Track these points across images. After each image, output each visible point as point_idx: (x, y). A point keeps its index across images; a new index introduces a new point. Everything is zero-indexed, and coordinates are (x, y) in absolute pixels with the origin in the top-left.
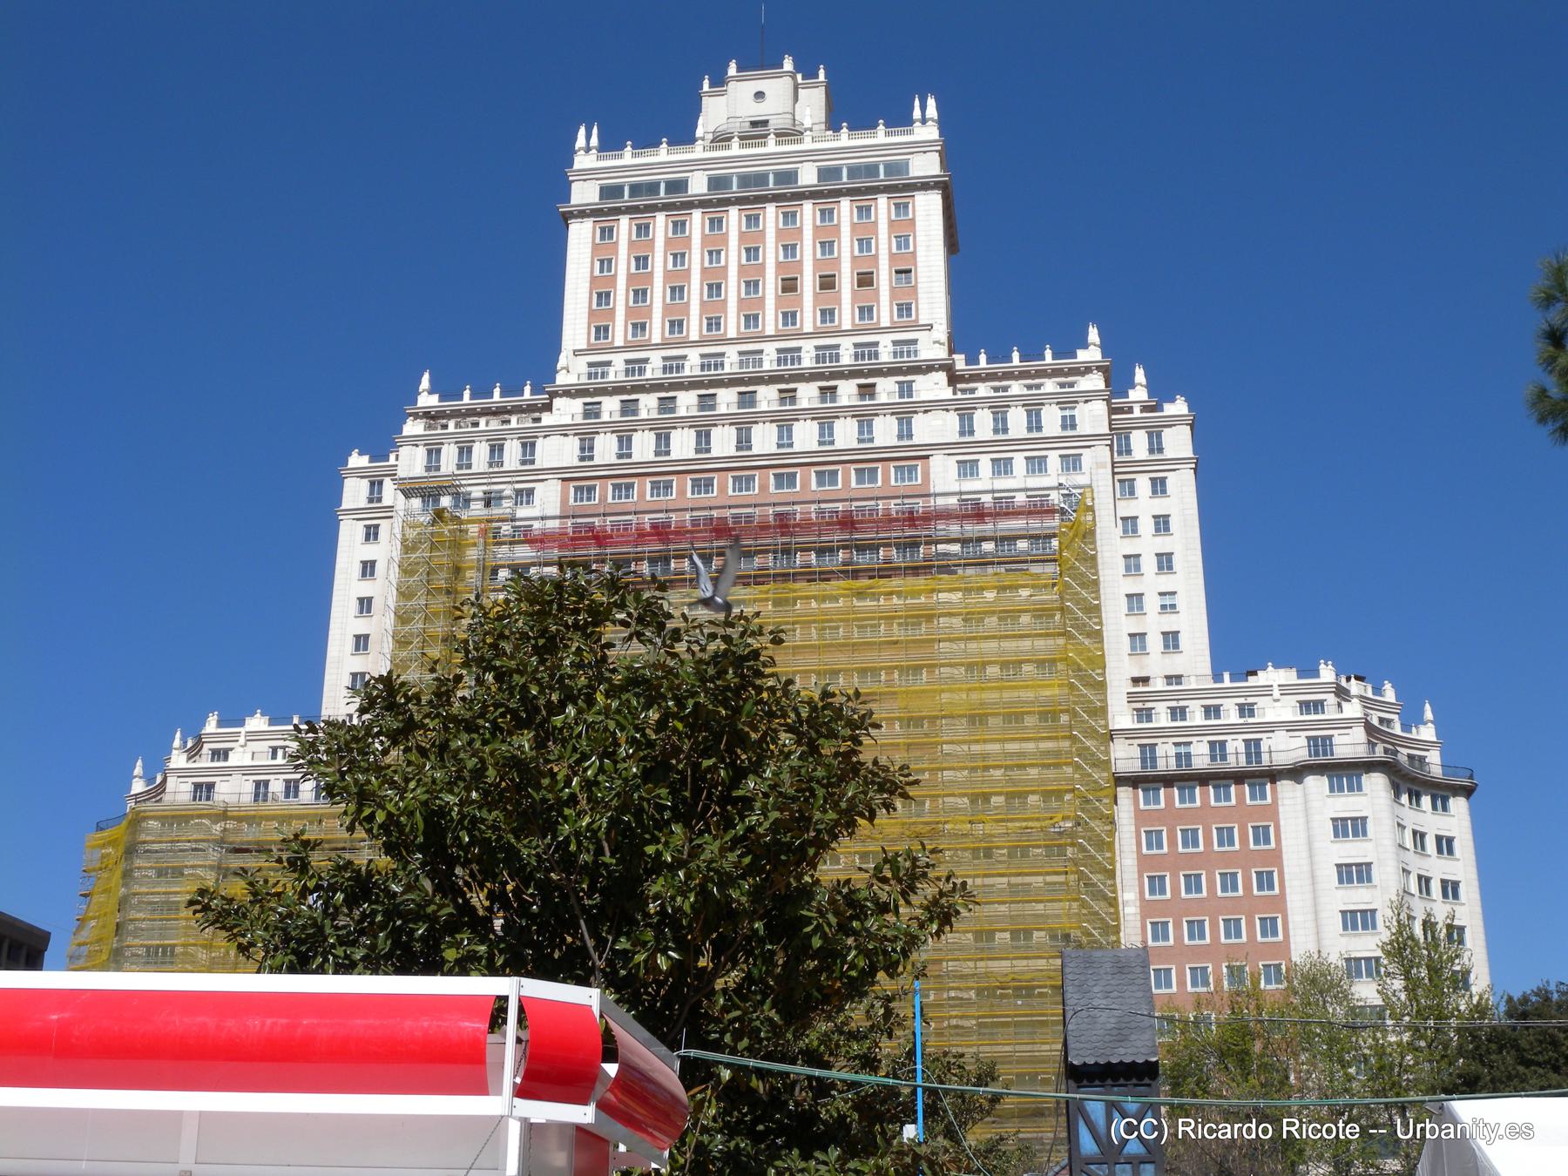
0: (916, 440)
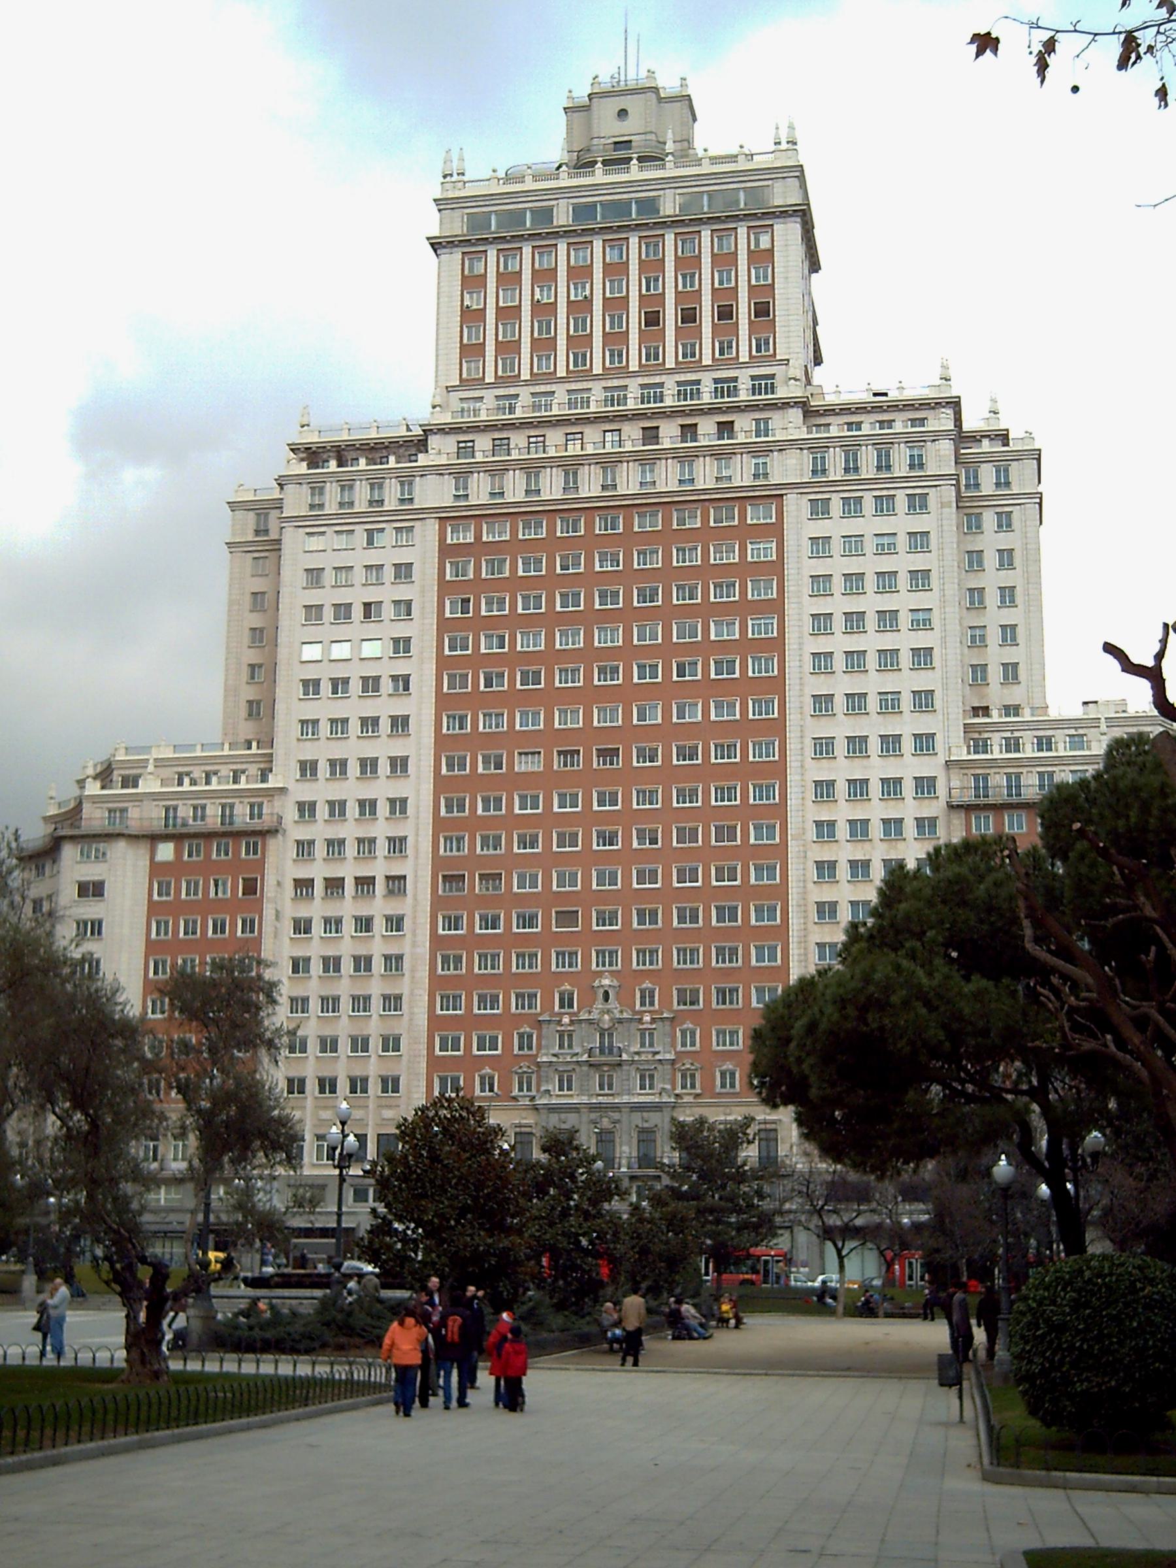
0: (774, 480)
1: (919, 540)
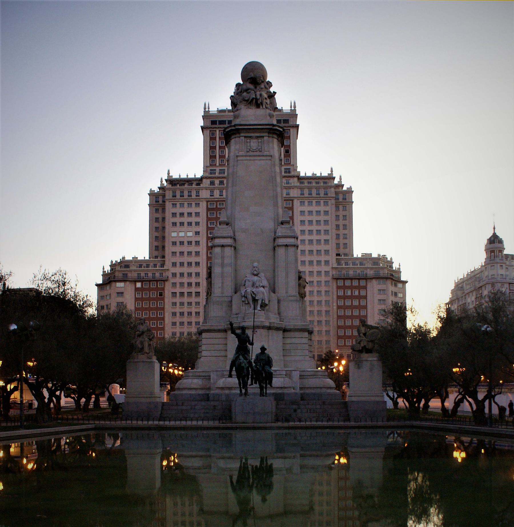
1: (326, 213)
